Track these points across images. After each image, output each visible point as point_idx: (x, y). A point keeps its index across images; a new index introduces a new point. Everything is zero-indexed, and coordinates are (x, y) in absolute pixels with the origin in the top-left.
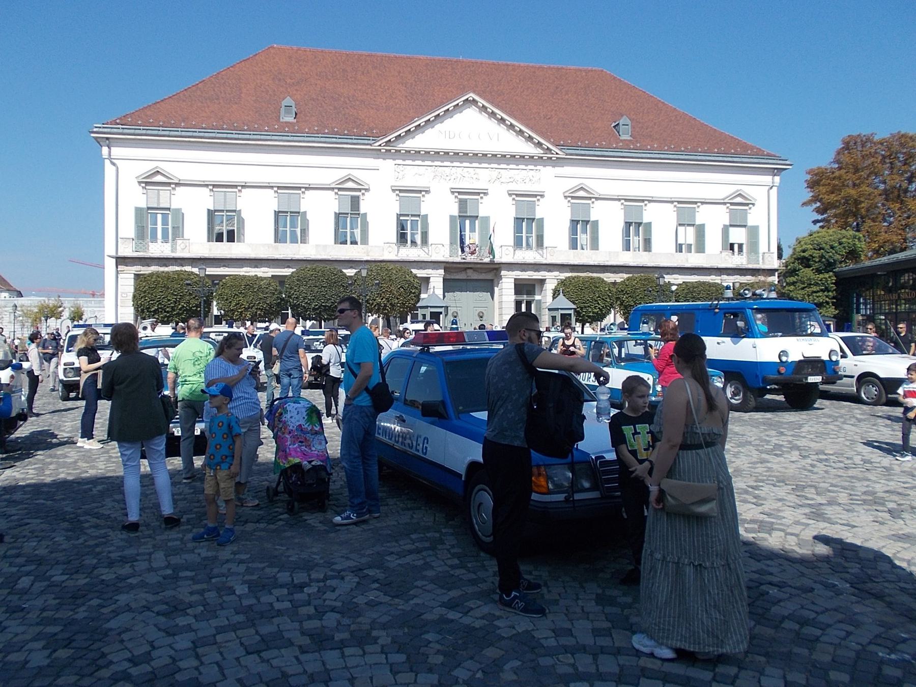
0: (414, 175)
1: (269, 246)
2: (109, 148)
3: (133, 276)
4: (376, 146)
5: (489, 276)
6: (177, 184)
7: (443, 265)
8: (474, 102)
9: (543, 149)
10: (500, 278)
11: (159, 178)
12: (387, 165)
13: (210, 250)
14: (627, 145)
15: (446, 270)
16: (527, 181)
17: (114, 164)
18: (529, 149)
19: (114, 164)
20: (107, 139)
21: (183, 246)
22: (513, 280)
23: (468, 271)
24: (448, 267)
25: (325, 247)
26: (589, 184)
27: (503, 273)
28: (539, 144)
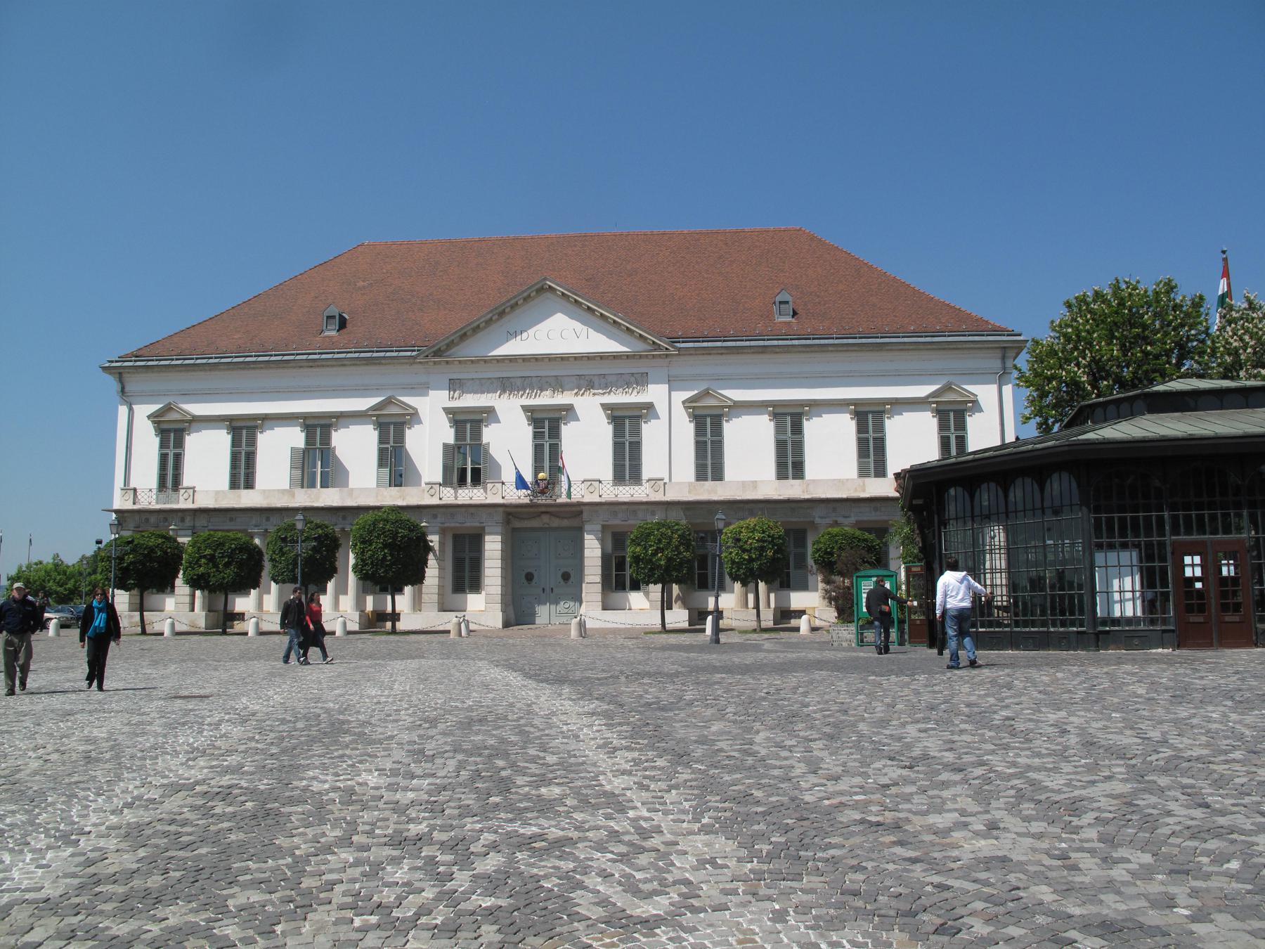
1: (283, 491)
5: (574, 523)
7: (501, 509)
21: (186, 496)
22: (599, 527)
27: (585, 516)
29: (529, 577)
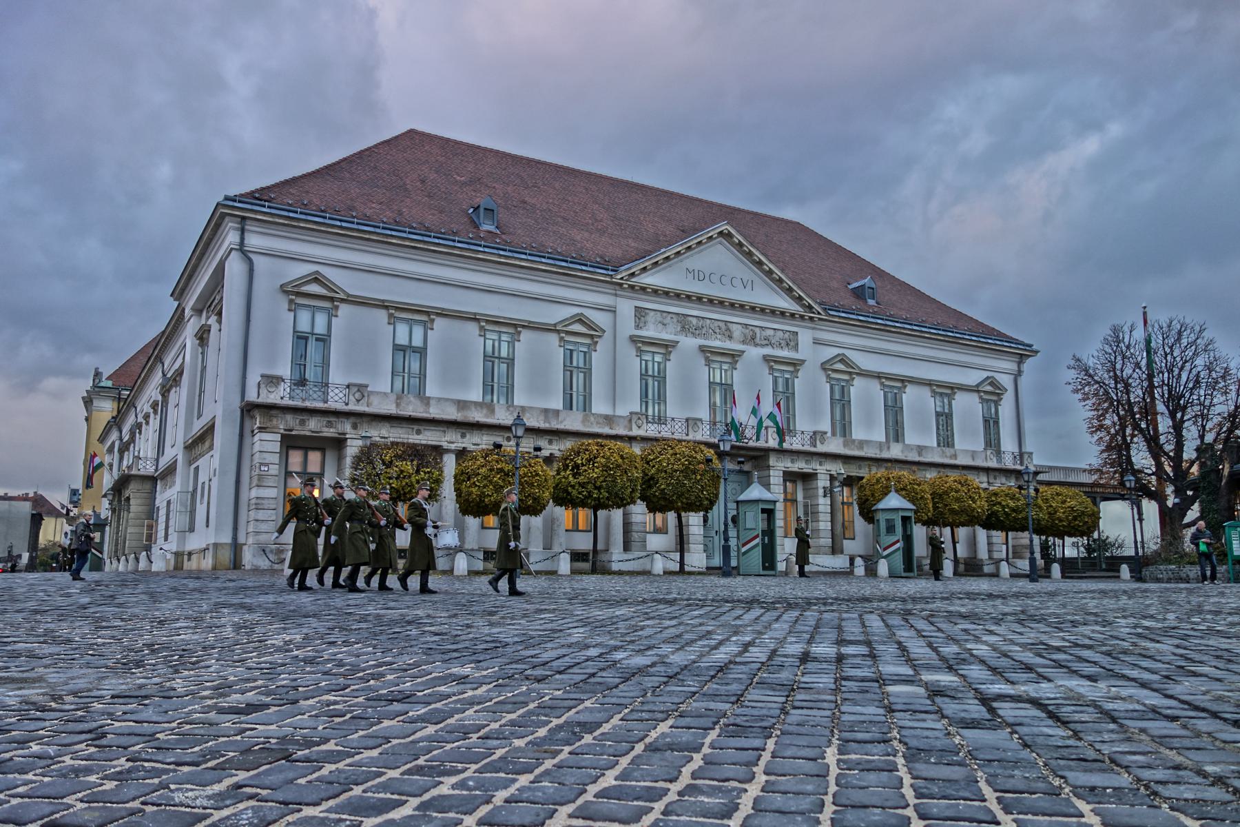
2: (243, 231)
6: (342, 300)
8: (728, 236)
9: (803, 306)
11: (314, 288)
16: (783, 343)
20: (244, 218)
26: (854, 356)
28: (799, 299)
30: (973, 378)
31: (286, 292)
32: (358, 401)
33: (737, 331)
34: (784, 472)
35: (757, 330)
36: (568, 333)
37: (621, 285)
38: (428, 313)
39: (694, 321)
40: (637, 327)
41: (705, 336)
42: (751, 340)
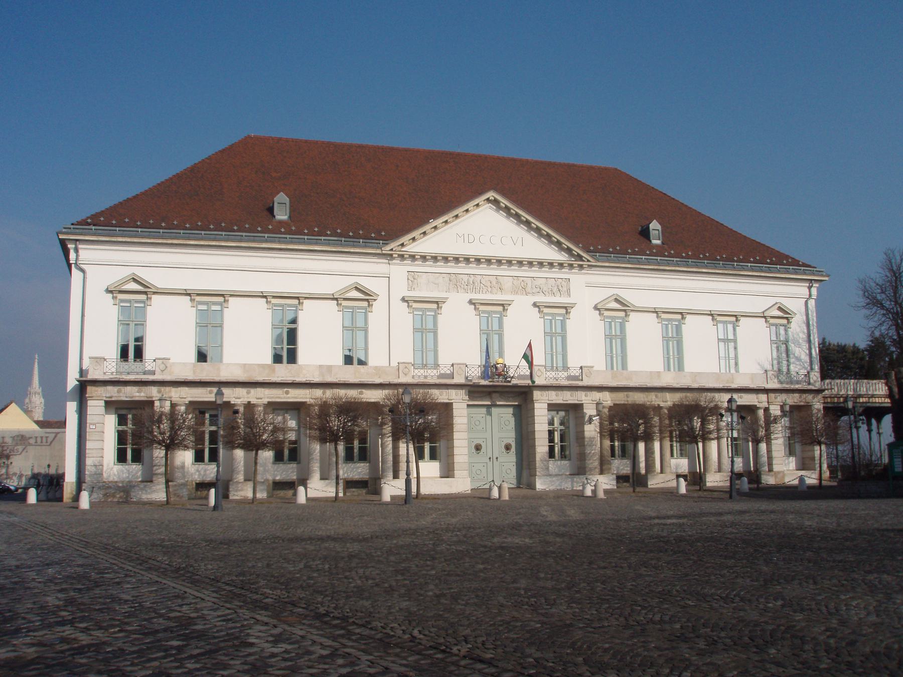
0: (431, 282)
1: (263, 366)
3: (103, 403)
4: (387, 249)
6: (155, 293)
10: (532, 401)
12: (399, 271)
13: (194, 372)
14: (660, 251)
15: (470, 392)
16: (555, 290)
17: (83, 271)
18: (562, 257)
19: (83, 271)
23: (494, 395)
24: (474, 391)
25: (329, 368)
28: (569, 251)
29: (478, 448)
30: (760, 305)
31: (111, 292)
32: (162, 371)
33: (507, 283)
34: (549, 405)
35: (529, 281)
36: (345, 299)
37: (391, 255)
38: (222, 295)
39: (466, 278)
40: (411, 288)
41: (474, 290)
42: (524, 291)
